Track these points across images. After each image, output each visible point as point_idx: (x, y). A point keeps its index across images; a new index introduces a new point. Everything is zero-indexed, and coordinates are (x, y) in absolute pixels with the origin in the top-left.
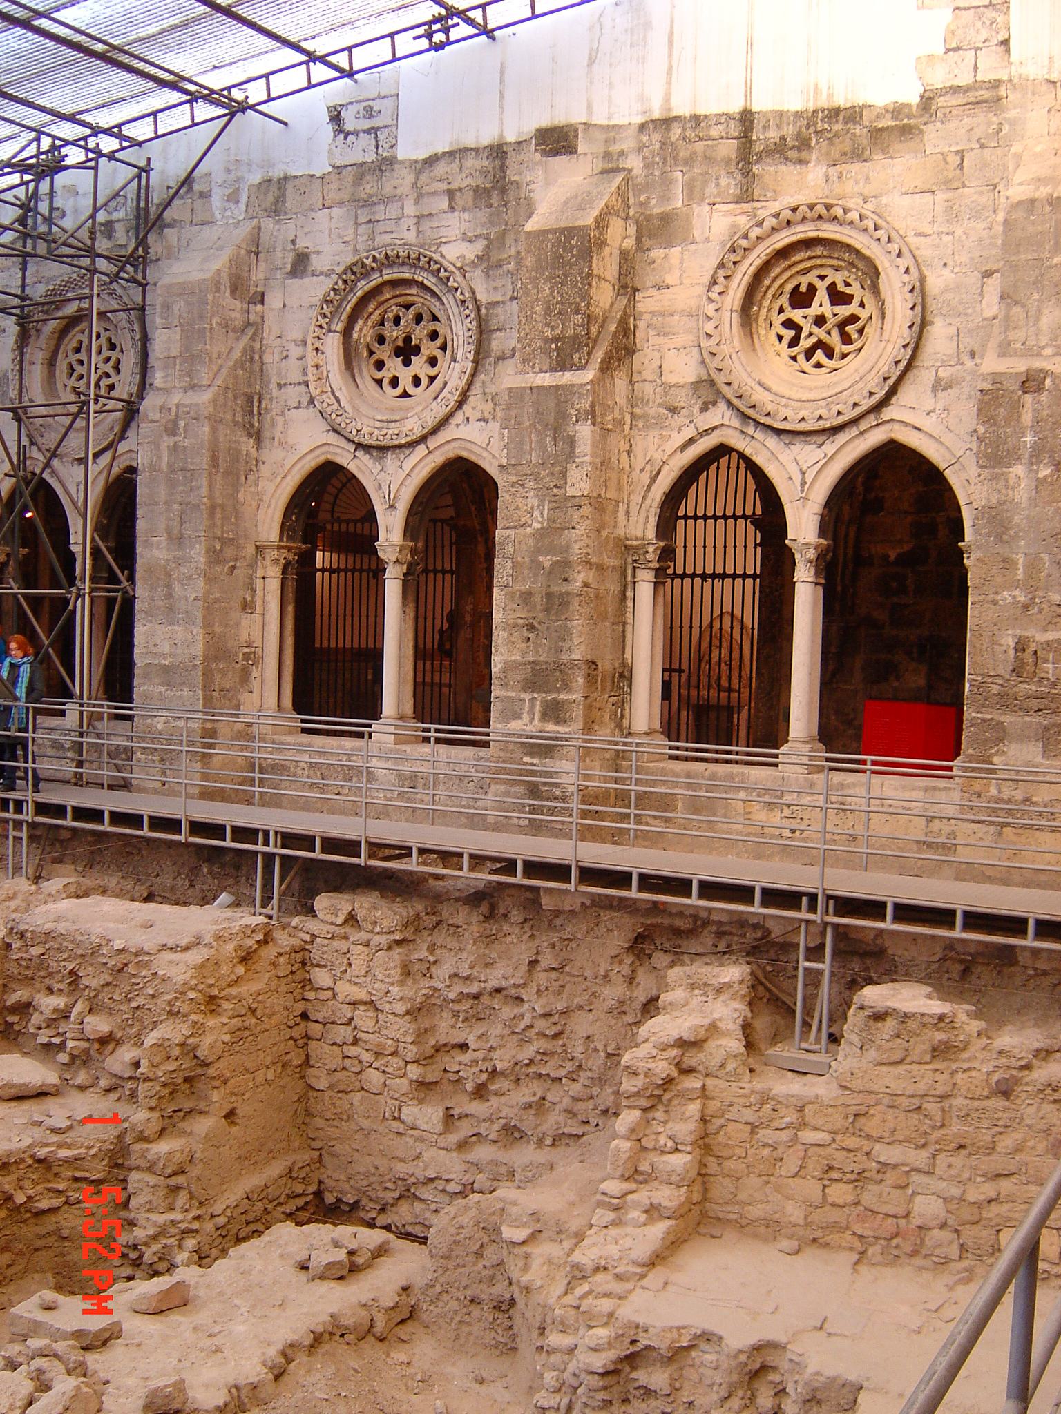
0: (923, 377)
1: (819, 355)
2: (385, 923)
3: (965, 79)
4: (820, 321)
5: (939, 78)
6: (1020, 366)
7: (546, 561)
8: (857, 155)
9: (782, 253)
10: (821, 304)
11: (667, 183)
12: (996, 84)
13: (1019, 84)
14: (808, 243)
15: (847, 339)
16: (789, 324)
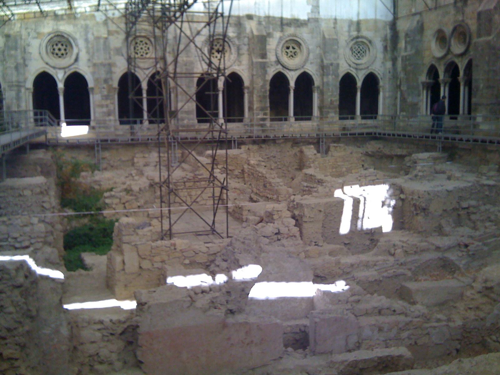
0: (309, 62)
1: (291, 57)
2: (255, 148)
3: (313, 17)
4: (291, 52)
5: (310, 16)
6: (329, 62)
7: (263, 90)
8: (299, 26)
9: (287, 41)
10: (291, 49)
11: (269, 27)
12: (318, 19)
13: (321, 19)
14: (290, 40)
15: (295, 55)
16: (286, 52)
